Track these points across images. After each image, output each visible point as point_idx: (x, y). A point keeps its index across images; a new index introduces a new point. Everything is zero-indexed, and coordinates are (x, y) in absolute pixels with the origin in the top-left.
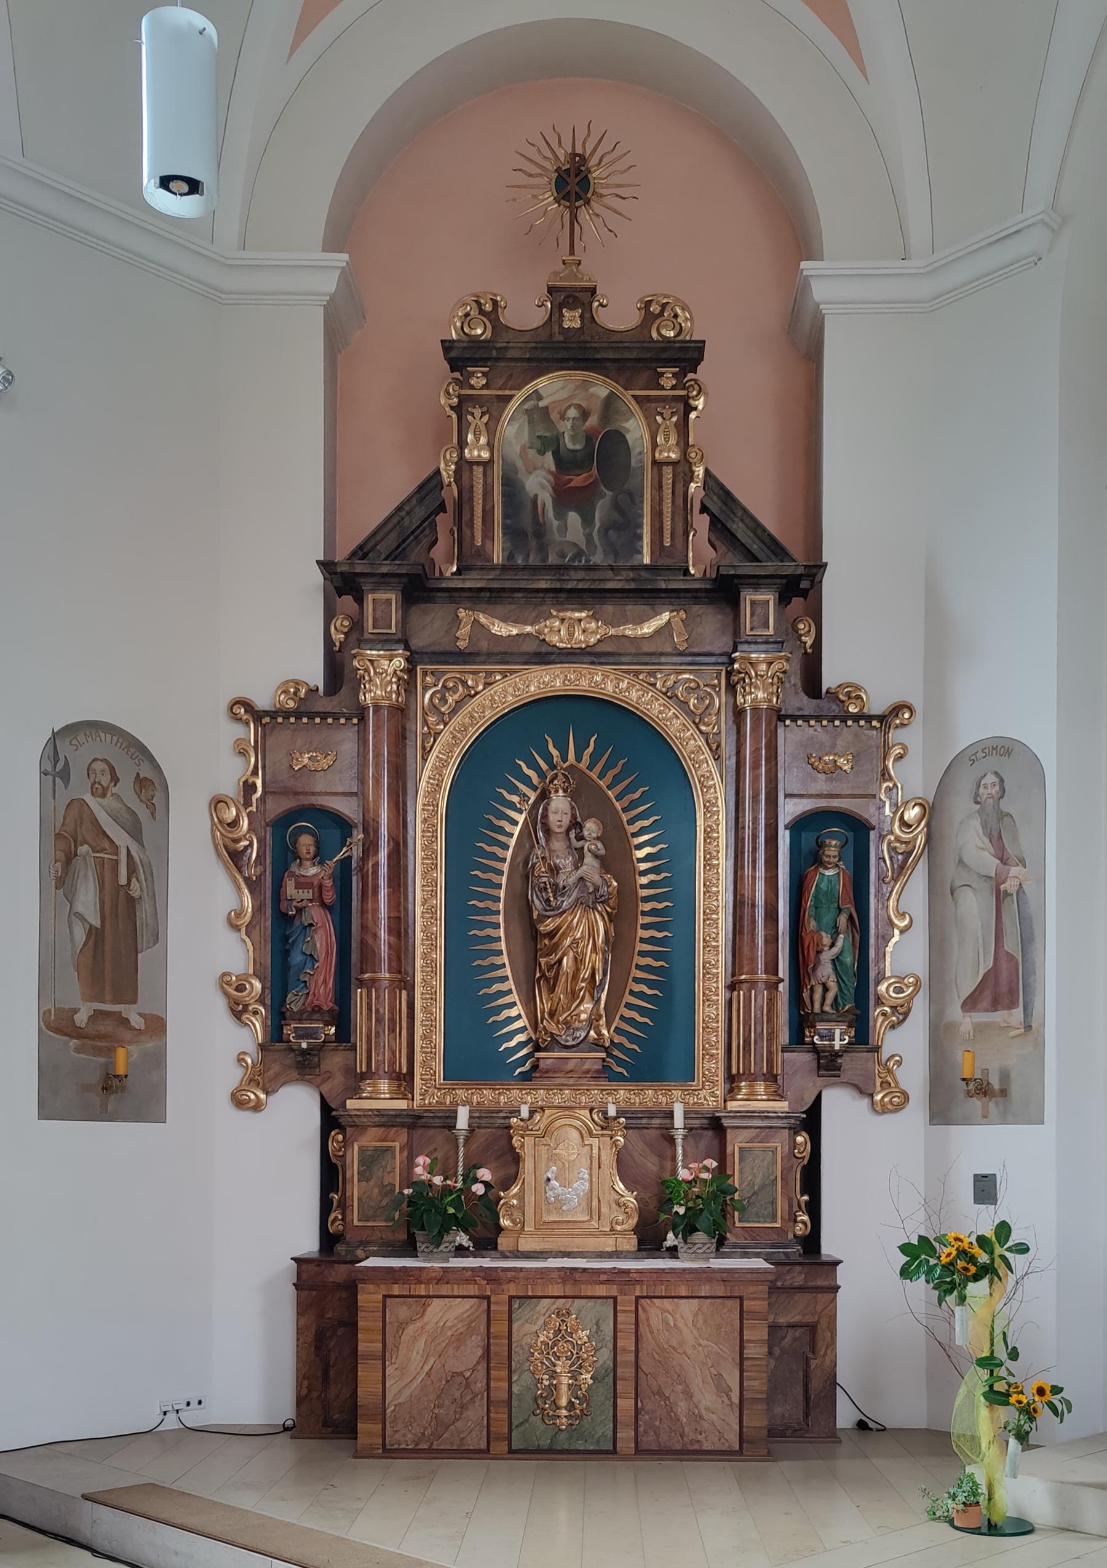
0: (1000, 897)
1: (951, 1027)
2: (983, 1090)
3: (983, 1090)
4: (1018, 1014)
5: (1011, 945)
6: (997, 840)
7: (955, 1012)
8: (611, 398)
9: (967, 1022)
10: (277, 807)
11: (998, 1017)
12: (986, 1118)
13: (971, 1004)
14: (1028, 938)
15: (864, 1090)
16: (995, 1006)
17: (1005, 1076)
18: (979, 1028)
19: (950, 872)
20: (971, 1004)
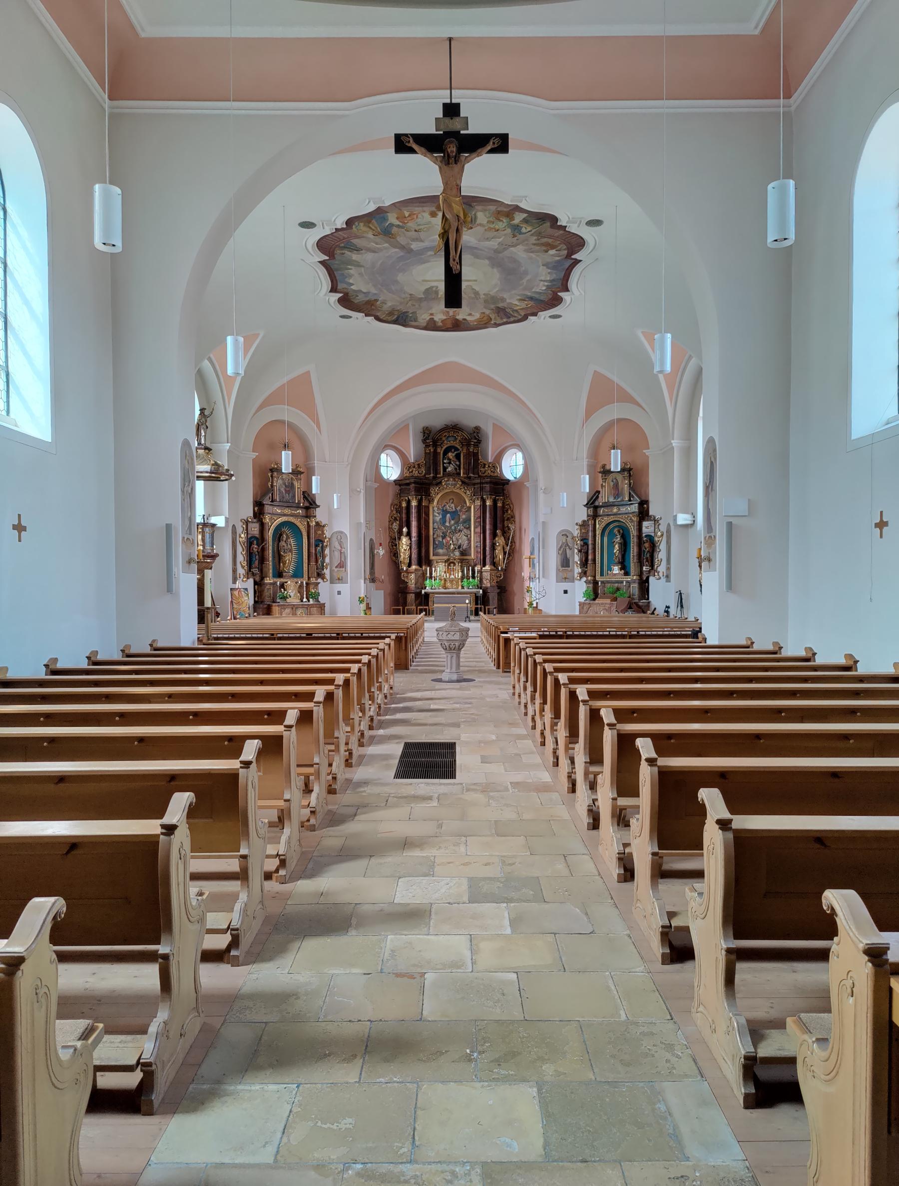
0: (341, 553)
1: (334, 570)
2: (339, 579)
3: (339, 579)
4: (344, 569)
5: (343, 559)
6: (340, 545)
7: (334, 568)
8: (292, 478)
9: (336, 570)
10: (249, 536)
11: (341, 569)
12: (339, 583)
13: (336, 567)
14: (345, 559)
15: (323, 579)
16: (340, 567)
17: (342, 577)
18: (338, 570)
19: (333, 549)
20: (336, 567)
